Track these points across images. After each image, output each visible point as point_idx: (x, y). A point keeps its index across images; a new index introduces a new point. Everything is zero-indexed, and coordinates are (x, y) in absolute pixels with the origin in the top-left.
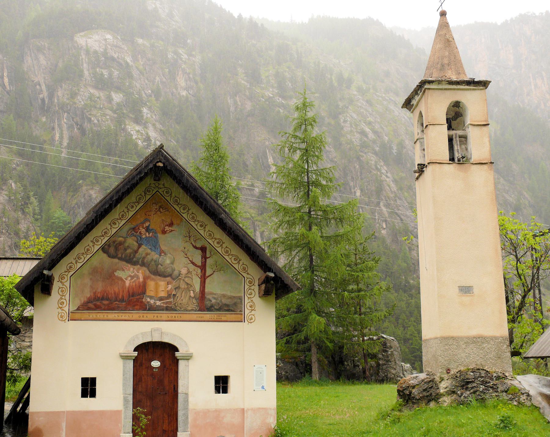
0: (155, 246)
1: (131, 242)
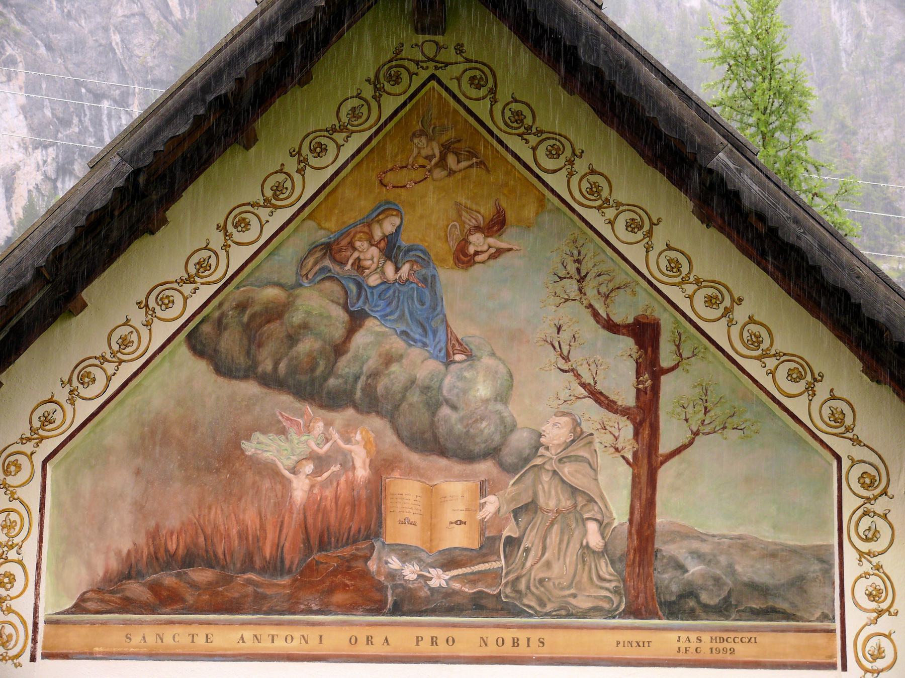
0: (425, 319)
1: (319, 306)
